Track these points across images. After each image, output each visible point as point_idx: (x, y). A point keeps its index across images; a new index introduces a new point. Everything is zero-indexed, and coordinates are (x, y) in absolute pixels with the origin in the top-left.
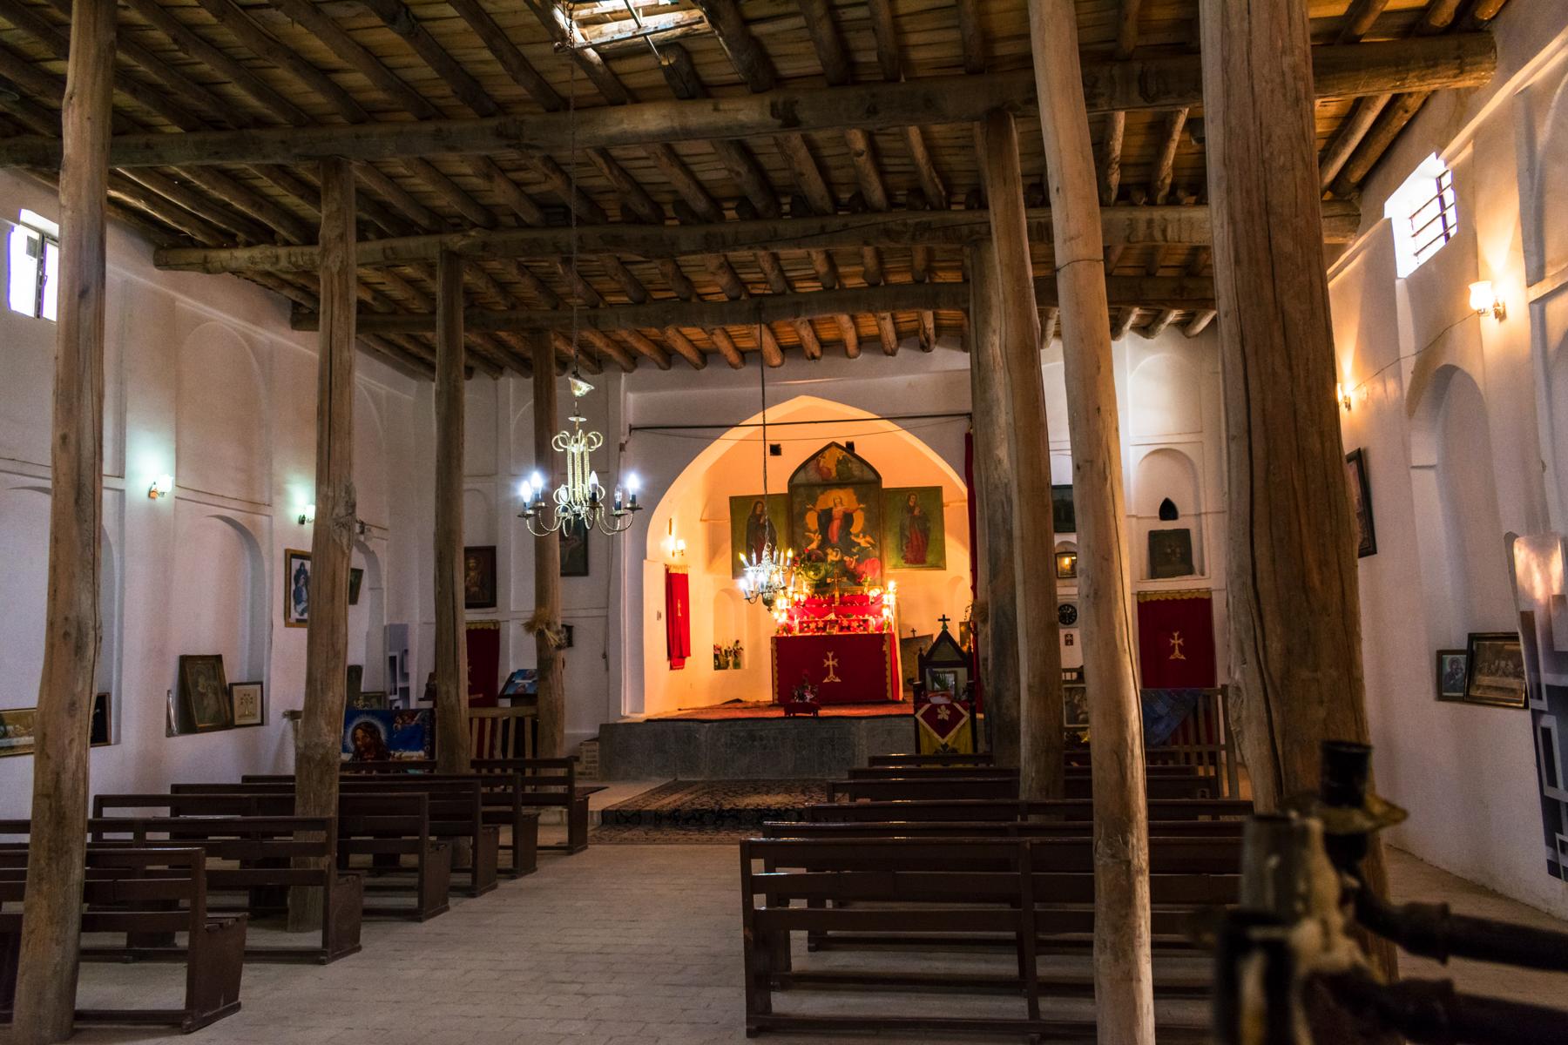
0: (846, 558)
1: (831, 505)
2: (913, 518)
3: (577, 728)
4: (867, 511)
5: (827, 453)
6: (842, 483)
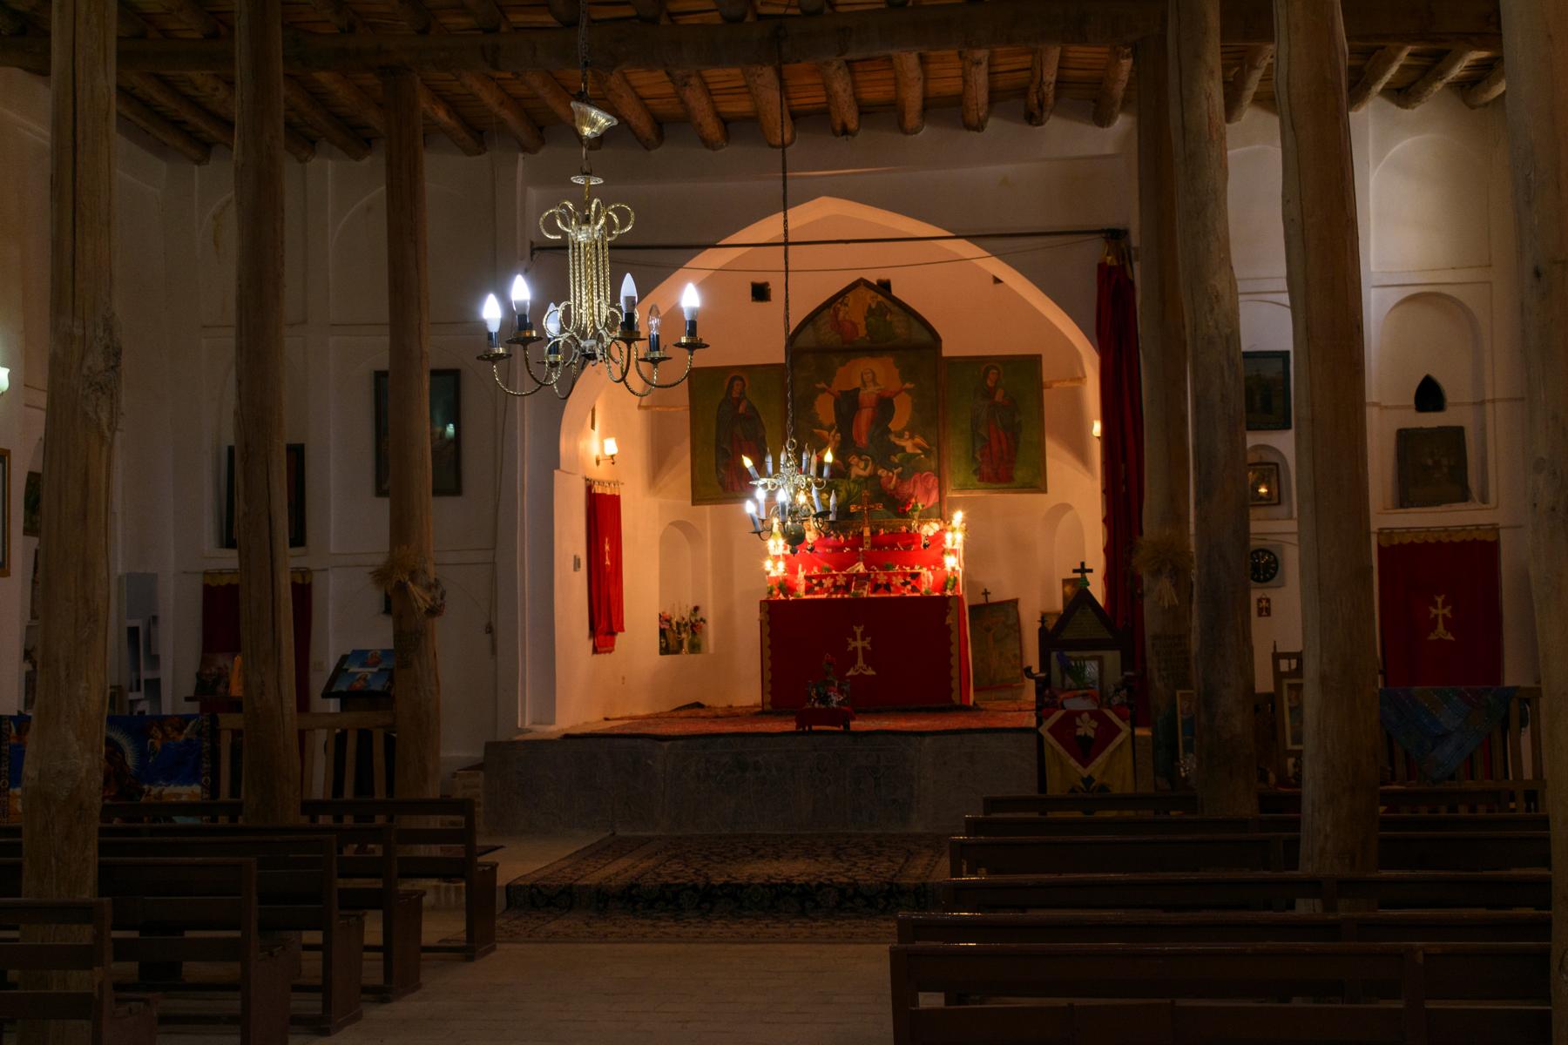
0: (882, 472)
1: (858, 383)
3: (456, 748)
5: (850, 295)
6: (873, 349)
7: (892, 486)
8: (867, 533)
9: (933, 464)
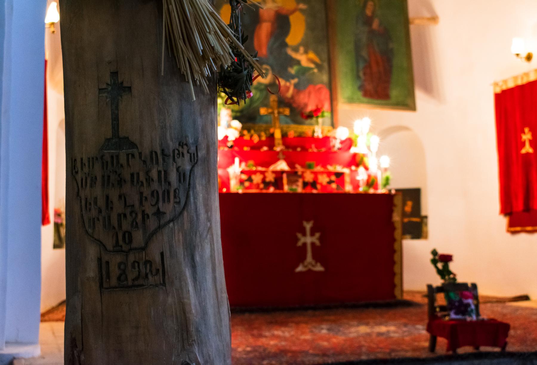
2: (372, 32)
4: (310, 14)
7: (290, 94)
8: (278, 135)
9: (325, 78)
